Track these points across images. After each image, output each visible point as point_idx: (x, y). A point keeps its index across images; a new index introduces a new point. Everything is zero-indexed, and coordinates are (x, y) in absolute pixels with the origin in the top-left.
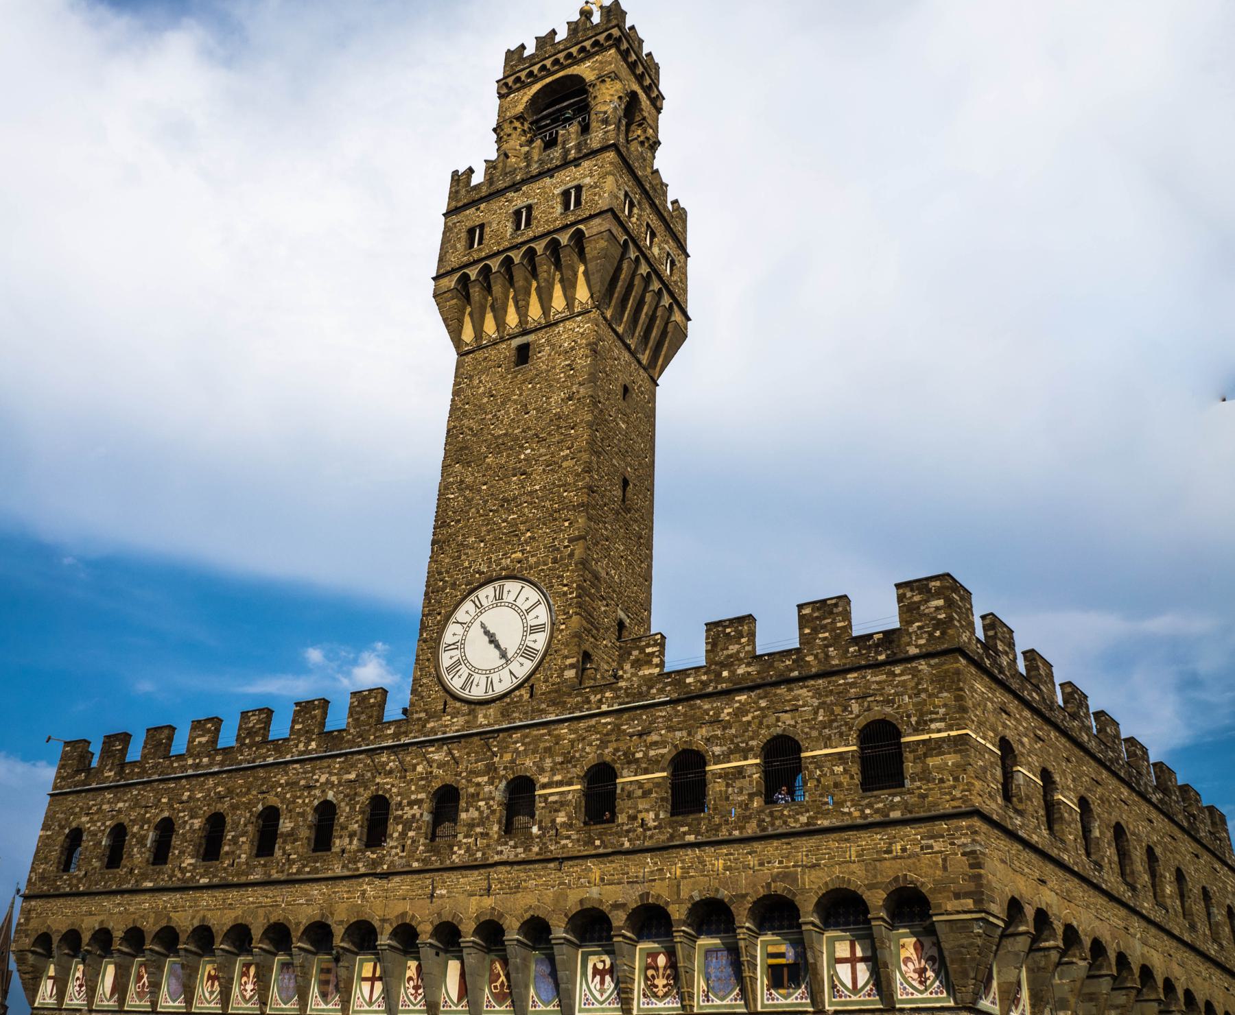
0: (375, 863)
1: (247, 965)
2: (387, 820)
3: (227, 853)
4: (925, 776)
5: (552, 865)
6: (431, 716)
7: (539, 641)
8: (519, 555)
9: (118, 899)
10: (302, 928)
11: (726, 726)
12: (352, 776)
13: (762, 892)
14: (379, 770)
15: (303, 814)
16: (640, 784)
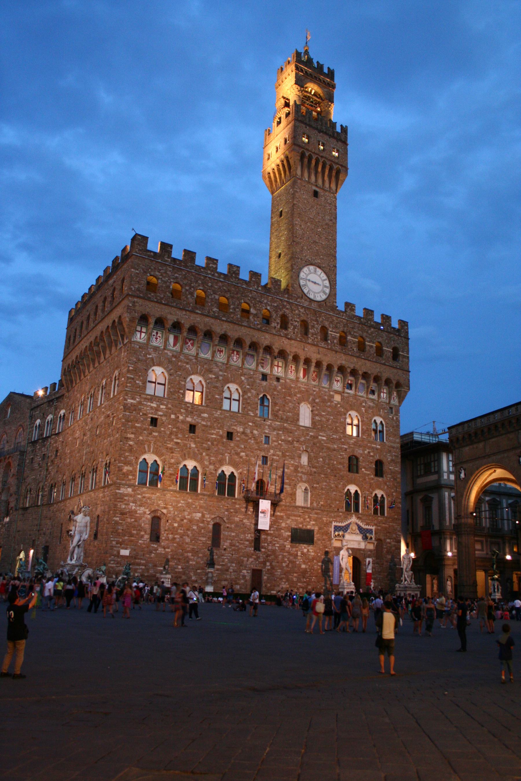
0: (286, 334)
1: (233, 351)
2: (288, 323)
3: (232, 312)
4: (402, 361)
5: (334, 352)
6: (299, 297)
7: (328, 291)
8: (319, 261)
9: (184, 313)
10: (264, 346)
11: (370, 335)
12: (275, 305)
13: (375, 374)
14: (284, 306)
15: (260, 310)
16: (353, 341)
